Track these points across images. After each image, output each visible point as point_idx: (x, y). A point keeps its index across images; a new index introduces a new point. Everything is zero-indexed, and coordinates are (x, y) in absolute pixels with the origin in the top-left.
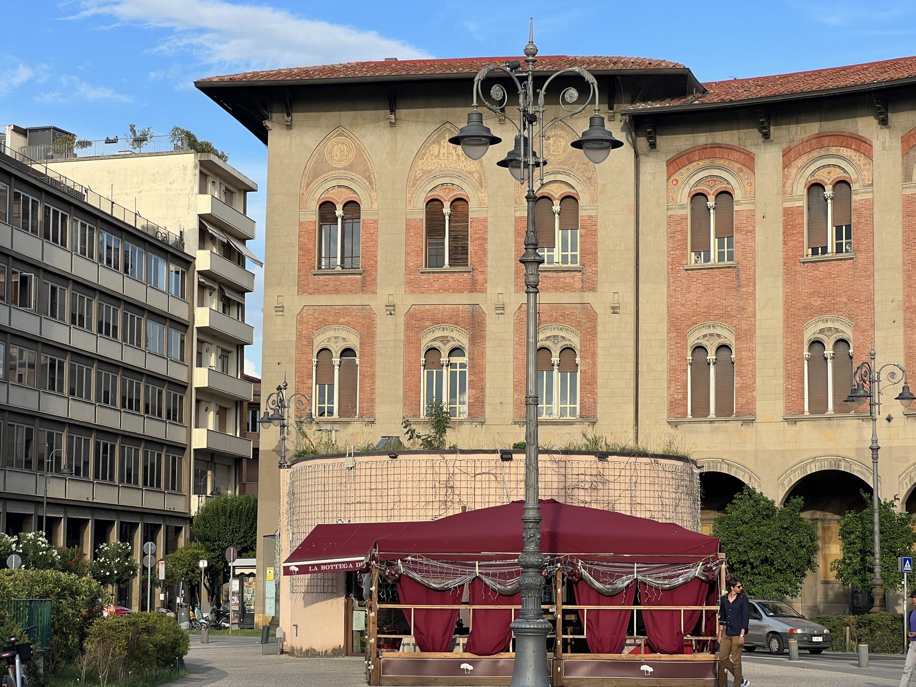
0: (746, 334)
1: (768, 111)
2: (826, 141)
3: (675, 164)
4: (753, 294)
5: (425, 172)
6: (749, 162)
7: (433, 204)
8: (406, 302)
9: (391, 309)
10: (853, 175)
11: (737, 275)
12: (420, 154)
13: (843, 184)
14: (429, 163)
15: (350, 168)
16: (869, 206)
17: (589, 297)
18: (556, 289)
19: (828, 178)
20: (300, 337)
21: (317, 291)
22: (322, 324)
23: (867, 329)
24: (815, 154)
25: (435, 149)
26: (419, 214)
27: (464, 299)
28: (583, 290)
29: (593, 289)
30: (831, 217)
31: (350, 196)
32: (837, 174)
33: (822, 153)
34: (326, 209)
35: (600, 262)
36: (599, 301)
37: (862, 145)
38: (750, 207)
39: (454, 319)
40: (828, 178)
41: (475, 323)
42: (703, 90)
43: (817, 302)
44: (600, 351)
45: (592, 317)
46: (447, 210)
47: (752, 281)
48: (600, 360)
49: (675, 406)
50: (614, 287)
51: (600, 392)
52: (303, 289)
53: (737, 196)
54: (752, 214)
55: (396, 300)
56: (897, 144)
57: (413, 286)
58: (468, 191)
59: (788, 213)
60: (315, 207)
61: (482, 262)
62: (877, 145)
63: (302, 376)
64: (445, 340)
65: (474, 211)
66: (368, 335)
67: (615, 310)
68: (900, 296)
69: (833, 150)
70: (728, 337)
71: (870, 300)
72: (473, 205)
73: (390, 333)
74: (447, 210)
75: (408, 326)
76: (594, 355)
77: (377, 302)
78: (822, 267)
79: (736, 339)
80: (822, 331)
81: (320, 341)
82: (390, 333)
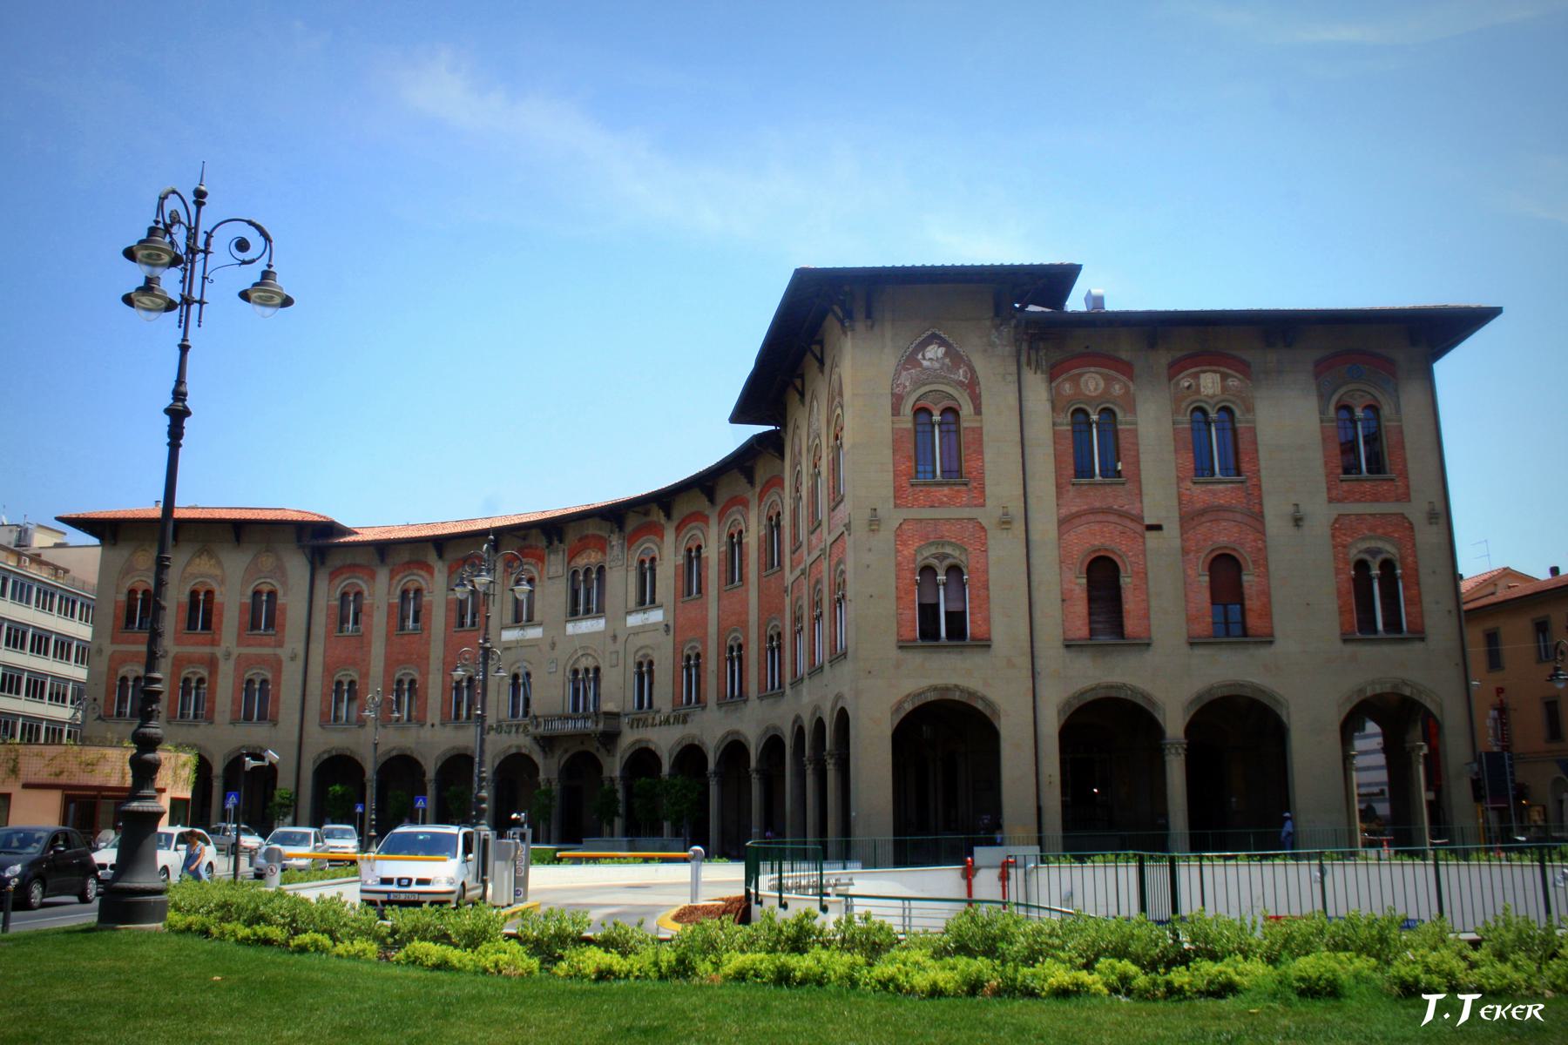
0: (365, 675)
1: (384, 549)
3: (334, 575)
6: (373, 576)
7: (194, 594)
10: (424, 585)
11: (362, 640)
12: (189, 563)
14: (194, 569)
16: (431, 603)
17: (279, 651)
20: (109, 668)
22: (123, 662)
23: (425, 674)
27: (206, 650)
30: (410, 606)
32: (416, 585)
36: (284, 653)
37: (429, 569)
39: (201, 661)
40: (412, 586)
41: (212, 664)
43: (402, 657)
45: (279, 662)
46: (201, 597)
47: (369, 644)
52: (114, 641)
53: (366, 593)
54: (372, 605)
56: (445, 570)
57: (178, 641)
58: (215, 586)
60: (125, 591)
61: (219, 629)
63: (109, 693)
65: (218, 598)
70: (356, 677)
72: (217, 594)
74: (201, 597)
75: (174, 665)
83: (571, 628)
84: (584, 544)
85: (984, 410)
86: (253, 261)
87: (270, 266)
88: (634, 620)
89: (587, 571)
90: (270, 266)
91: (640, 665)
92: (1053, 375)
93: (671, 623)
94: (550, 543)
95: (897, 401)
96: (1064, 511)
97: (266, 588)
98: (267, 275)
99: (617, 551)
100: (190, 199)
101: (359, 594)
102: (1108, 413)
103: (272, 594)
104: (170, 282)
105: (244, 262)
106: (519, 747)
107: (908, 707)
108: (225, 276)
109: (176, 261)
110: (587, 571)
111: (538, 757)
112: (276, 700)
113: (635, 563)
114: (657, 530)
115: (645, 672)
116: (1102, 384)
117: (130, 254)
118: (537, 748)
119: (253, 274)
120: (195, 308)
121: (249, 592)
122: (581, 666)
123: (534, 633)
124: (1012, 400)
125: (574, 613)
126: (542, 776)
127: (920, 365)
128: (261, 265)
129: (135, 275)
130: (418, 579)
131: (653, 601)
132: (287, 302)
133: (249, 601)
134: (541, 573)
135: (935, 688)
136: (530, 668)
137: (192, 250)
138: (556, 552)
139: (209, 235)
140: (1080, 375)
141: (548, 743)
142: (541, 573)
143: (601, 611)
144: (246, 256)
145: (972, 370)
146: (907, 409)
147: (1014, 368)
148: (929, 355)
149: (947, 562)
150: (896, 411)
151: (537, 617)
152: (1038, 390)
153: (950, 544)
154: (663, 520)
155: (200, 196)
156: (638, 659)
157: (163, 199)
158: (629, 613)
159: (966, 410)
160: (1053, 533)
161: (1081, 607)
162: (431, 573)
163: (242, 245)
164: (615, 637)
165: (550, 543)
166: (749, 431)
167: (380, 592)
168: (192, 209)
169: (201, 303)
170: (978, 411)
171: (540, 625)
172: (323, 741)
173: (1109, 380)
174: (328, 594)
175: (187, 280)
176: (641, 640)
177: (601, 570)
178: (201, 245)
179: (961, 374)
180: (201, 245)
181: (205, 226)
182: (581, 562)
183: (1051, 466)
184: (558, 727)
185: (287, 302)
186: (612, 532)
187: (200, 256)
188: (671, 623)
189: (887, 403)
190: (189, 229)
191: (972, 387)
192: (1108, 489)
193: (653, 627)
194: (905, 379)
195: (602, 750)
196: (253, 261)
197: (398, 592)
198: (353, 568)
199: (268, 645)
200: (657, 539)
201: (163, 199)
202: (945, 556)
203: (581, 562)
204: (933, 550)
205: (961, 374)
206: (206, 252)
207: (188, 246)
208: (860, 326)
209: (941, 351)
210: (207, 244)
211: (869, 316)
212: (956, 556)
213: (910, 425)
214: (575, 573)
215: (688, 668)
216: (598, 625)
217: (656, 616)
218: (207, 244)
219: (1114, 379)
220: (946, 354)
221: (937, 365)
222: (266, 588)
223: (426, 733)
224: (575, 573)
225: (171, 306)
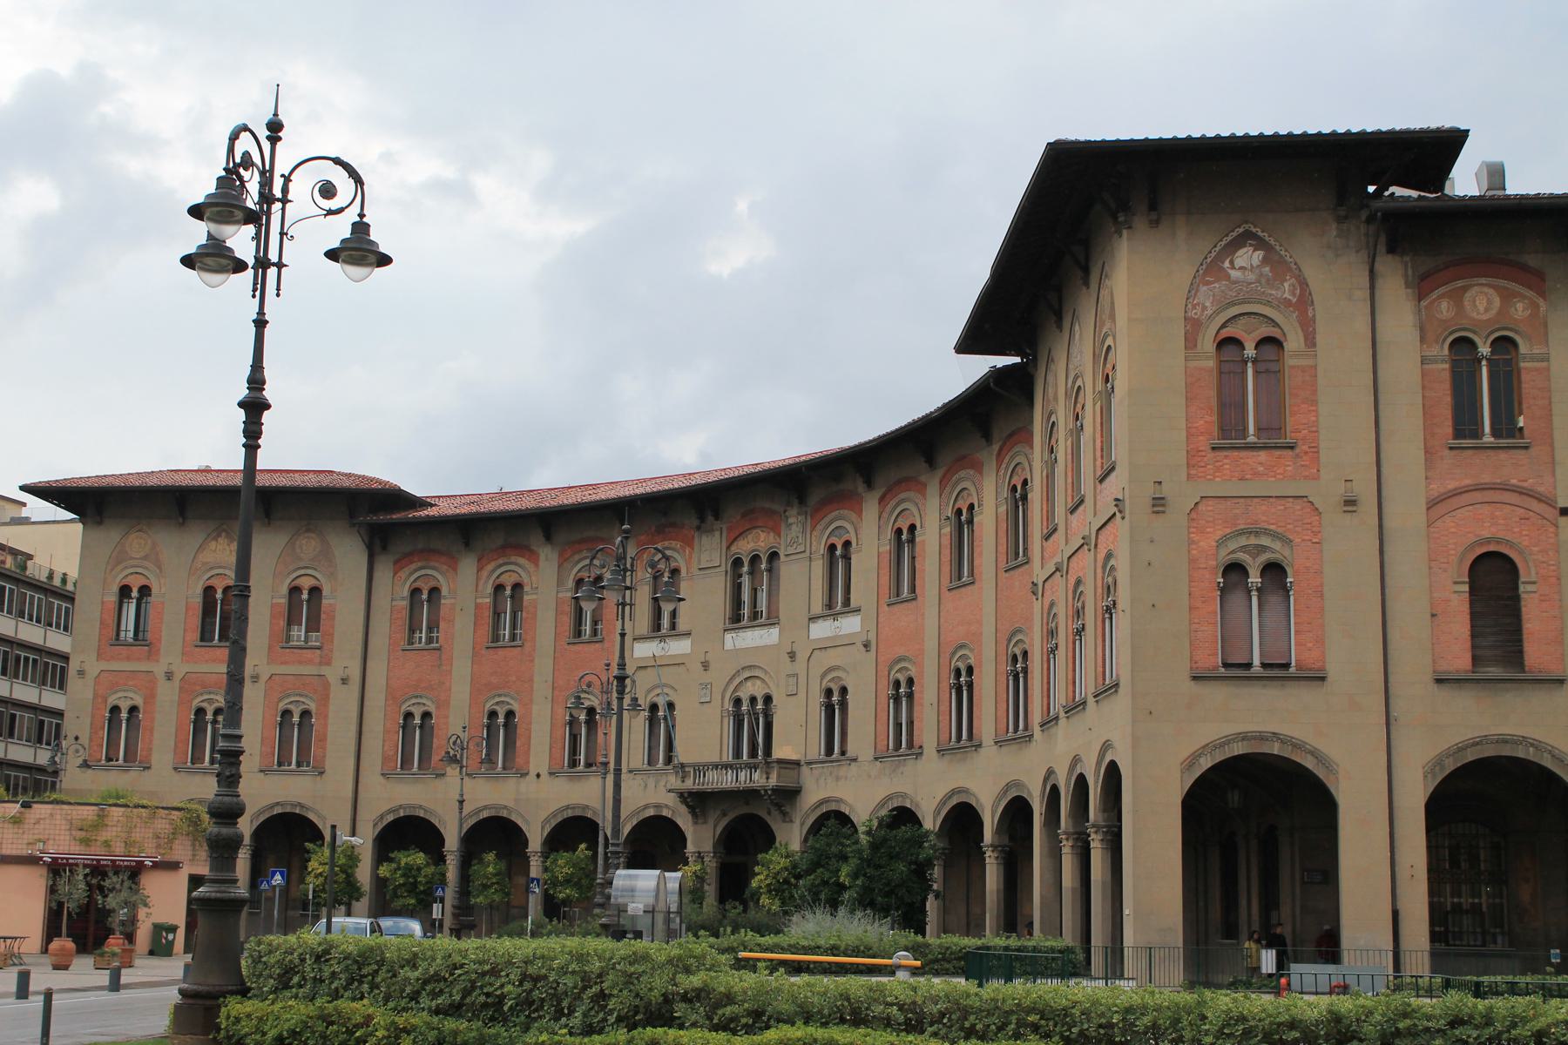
0: (443, 704)
4: (450, 672)
5: (204, 564)
8: (180, 670)
9: (169, 676)
10: (525, 579)
12: (201, 548)
15: (145, 558)
17: (325, 670)
18: (300, 662)
19: (508, 580)
20: (96, 696)
21: (112, 658)
24: (501, 561)
25: (213, 545)
26: (197, 600)
28: (321, 664)
29: (328, 663)
31: (143, 582)
34: (125, 591)
35: (336, 642)
36: (332, 674)
37: (533, 557)
40: (508, 580)
44: (331, 715)
45: (326, 686)
46: (219, 595)
48: (330, 721)
49: (386, 759)
50: (345, 660)
51: (329, 747)
52: (100, 657)
53: (444, 591)
55: (173, 668)
59: (478, 607)
62: (542, 557)
64: (210, 701)
66: (150, 697)
67: (344, 681)
69: (513, 559)
70: (431, 708)
71: (531, 680)
73: (167, 695)
74: (219, 595)
76: (326, 717)
77: (159, 669)
78: (501, 652)
79: (438, 708)
81: (112, 700)
82: (167, 695)
85: (1319, 339)
86: (340, 211)
87: (362, 215)
88: (822, 630)
89: (755, 559)
90: (362, 215)
91: (829, 692)
92: (1422, 286)
93: (872, 637)
94: (702, 519)
95: (1193, 329)
96: (1437, 488)
97: (306, 583)
98: (361, 228)
99: (795, 530)
100: (263, 133)
101: (435, 591)
102: (1504, 344)
103: (315, 591)
104: (241, 241)
105: (330, 212)
106: (657, 806)
107: (1206, 763)
108: (309, 232)
109: (251, 217)
110: (755, 559)
111: (684, 821)
112: (323, 739)
113: (822, 549)
114: (849, 500)
115: (835, 705)
116: (1497, 302)
117: (196, 212)
118: (683, 809)
119: (340, 230)
120: (272, 272)
121: (284, 590)
123: (679, 647)
124: (1362, 325)
127: (1228, 277)
128: (352, 215)
129: (197, 234)
130: (517, 569)
131: (847, 602)
132: (384, 260)
133: (284, 601)
134: (688, 563)
135: (1244, 737)
136: (673, 697)
137: (266, 198)
138: (711, 531)
139: (287, 179)
140: (1465, 289)
141: (698, 802)
142: (688, 563)
143: (773, 620)
144: (333, 204)
145: (1303, 284)
146: (1207, 343)
147: (1364, 280)
148: (1239, 262)
149: (1264, 558)
150: (1191, 341)
151: (682, 625)
152: (1400, 315)
153: (1267, 532)
154: (861, 488)
155: (275, 127)
157: (234, 137)
158: (813, 619)
159: (1294, 342)
160: (1420, 517)
161: (1460, 626)
162: (536, 562)
163: (328, 191)
164: (792, 655)
165: (702, 519)
166: (980, 366)
167: (465, 586)
168: (266, 146)
169: (280, 265)
170: (1310, 341)
171: (688, 634)
172: (390, 796)
173: (1507, 297)
174: (393, 587)
175: (261, 239)
176: (832, 658)
177: (774, 556)
178: (277, 192)
179: (1287, 290)
180: (277, 192)
181: (282, 167)
182: (745, 547)
183: (1419, 421)
185: (384, 260)
186: (789, 504)
187: (277, 206)
188: (872, 637)
189: (1179, 331)
190: (263, 173)
191: (1303, 303)
192: (1503, 455)
194: (1206, 297)
195: (775, 813)
196: (340, 211)
197: (490, 589)
198: (428, 553)
199: (310, 662)
200: (853, 516)
201: (234, 137)
202: (1263, 549)
203: (745, 547)
204: (1243, 541)
205: (1287, 290)
206: (285, 201)
207: (261, 194)
208: (1140, 223)
209: (1259, 255)
210: (285, 190)
211: (1153, 207)
212: (1278, 551)
213: (1211, 363)
214: (737, 563)
215: (897, 699)
217: (850, 625)
218: (285, 190)
219: (1515, 295)
220: (1265, 261)
221: (1251, 277)
222: (306, 583)
223: (528, 786)
224: (737, 563)
225: (240, 266)
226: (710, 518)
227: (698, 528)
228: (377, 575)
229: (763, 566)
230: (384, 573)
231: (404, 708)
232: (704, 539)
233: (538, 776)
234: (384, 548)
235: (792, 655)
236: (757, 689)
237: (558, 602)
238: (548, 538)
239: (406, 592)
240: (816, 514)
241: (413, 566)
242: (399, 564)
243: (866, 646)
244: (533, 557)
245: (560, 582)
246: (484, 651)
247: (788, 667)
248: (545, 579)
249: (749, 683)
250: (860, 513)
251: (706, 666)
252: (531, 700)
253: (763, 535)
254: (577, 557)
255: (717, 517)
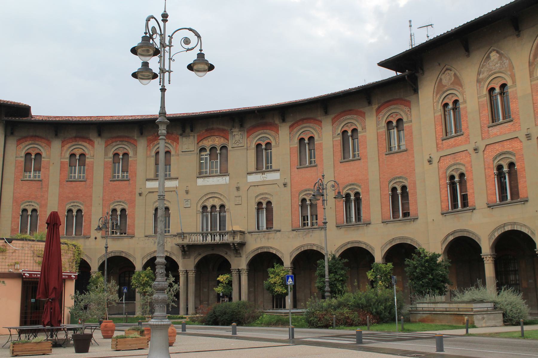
2: (78, 139)
4: (47, 191)
13: (82, 155)
19: (78, 152)
24: (74, 143)
32: (81, 151)
33: (76, 143)
37: (91, 142)
38: (48, 160)
40: (78, 152)
42: (32, 117)
43: (71, 196)
53: (44, 155)
54: (49, 162)
68: (101, 196)
69: (80, 143)
70: (37, 207)
71: (91, 196)
79: (40, 207)
80: (72, 206)
83: (200, 182)
84: (210, 132)
99: (237, 137)
101: (38, 155)
113: (254, 146)
122: (209, 204)
125: (201, 175)
126: (181, 269)
141: (187, 250)
143: (224, 173)
156: (258, 200)
158: (249, 174)
162: (93, 145)
164: (238, 189)
165: (184, 131)
167: (55, 153)
177: (224, 147)
182: (208, 143)
184: (199, 240)
188: (288, 181)
193: (273, 183)
197: (68, 155)
198: (35, 137)
200: (273, 133)
216: (224, 180)
226: (188, 130)
227: (181, 135)
228: (8, 145)
229: (218, 151)
230: (12, 145)
231: (22, 207)
232: (184, 139)
233: (96, 238)
234: (12, 134)
235: (238, 189)
236: (217, 203)
237: (106, 163)
238: (100, 135)
239: (23, 154)
240: (250, 132)
241: (27, 143)
242: (20, 141)
243: (285, 185)
244: (91, 142)
245: (106, 154)
246: (65, 183)
247: (236, 193)
248: (98, 153)
249: (211, 200)
250: (277, 132)
251: (187, 192)
252: (91, 205)
253: (217, 139)
254: (114, 144)
255: (192, 131)
